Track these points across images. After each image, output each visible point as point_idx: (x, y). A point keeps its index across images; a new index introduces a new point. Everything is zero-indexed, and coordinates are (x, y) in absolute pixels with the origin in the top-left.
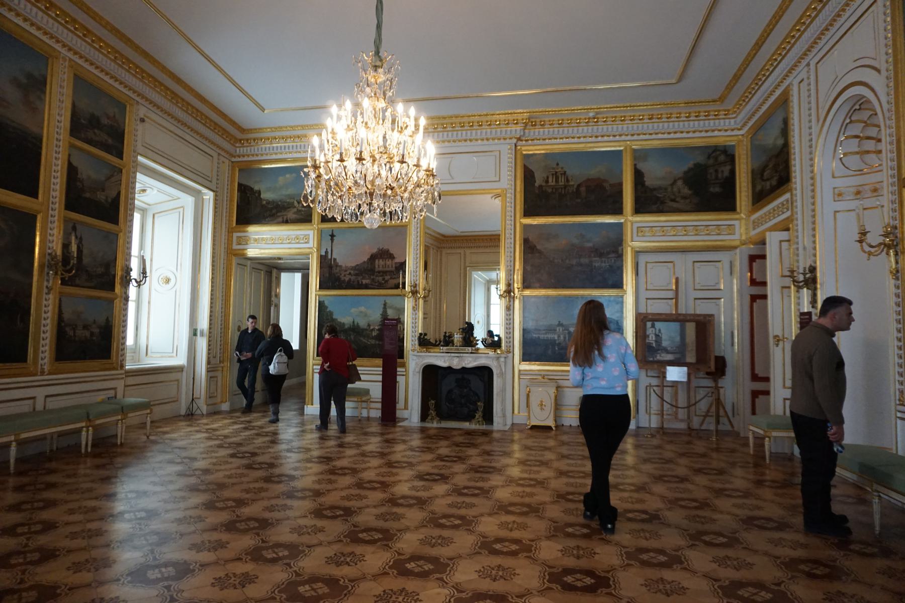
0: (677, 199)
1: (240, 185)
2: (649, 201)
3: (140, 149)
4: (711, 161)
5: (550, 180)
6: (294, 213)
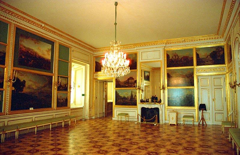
1: (96, 62)
2: (200, 62)
3: (73, 58)
4: (217, 50)
5: (174, 57)
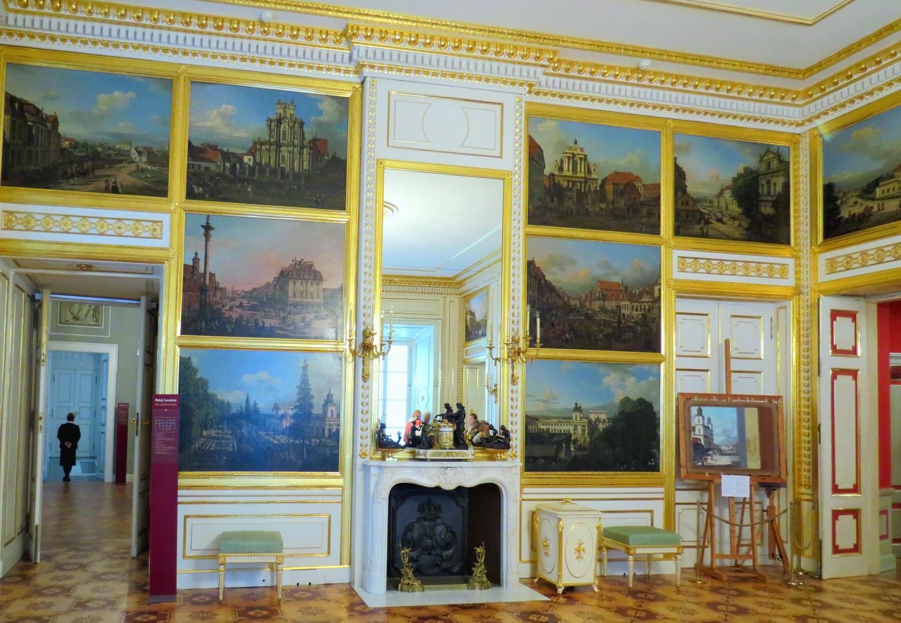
0: (725, 219)
1: (11, 100)
2: (693, 220)
6: (130, 174)
